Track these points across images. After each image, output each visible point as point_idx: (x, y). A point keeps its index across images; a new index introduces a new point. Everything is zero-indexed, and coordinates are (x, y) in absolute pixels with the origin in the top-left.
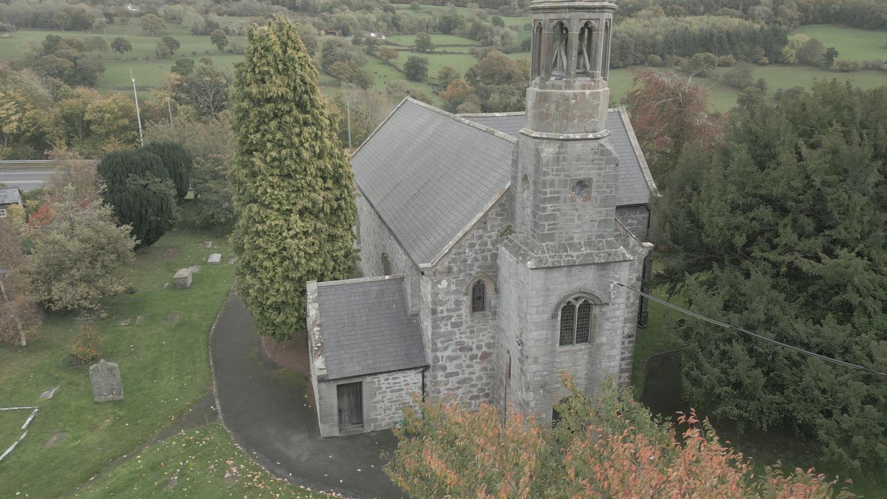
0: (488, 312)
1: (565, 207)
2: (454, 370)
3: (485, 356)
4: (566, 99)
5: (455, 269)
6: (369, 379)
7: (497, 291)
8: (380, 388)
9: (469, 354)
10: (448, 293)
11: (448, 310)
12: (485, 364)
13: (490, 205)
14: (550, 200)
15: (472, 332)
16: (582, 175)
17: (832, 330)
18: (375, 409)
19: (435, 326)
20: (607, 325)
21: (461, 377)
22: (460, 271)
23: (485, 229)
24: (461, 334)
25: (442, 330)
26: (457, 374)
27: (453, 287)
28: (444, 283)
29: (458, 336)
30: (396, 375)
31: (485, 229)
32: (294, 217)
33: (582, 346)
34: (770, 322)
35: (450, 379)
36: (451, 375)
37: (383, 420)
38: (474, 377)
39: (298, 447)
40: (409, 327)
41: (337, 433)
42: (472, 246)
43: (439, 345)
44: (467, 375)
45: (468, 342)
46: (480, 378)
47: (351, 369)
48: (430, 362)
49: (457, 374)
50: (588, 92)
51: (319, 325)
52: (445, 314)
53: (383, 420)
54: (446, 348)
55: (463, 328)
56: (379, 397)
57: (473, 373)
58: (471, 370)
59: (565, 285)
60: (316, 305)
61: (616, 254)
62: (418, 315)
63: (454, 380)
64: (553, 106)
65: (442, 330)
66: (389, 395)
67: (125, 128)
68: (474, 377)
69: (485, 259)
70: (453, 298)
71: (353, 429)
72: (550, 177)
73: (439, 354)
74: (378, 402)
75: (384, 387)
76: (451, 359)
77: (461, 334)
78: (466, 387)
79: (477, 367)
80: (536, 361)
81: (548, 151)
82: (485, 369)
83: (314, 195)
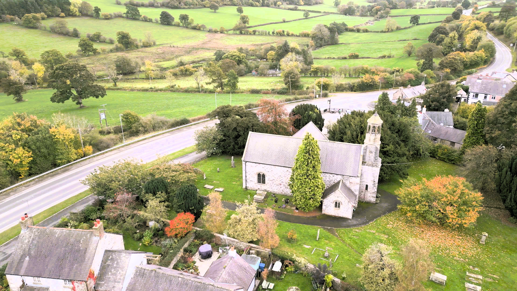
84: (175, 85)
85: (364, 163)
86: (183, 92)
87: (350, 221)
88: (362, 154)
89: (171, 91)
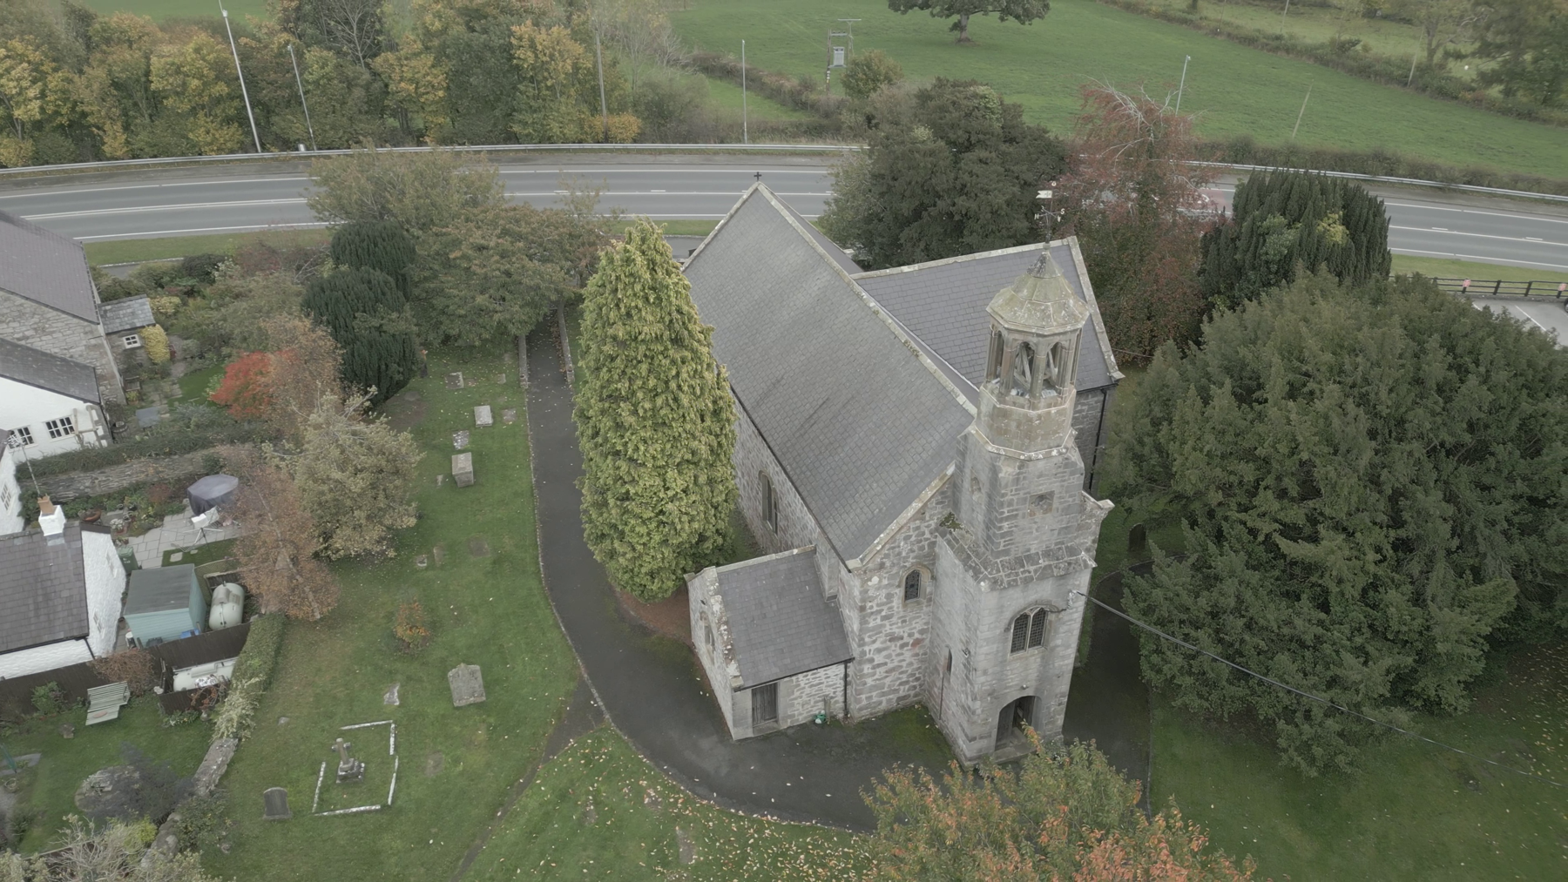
1: (1022, 522)
3: (917, 642)
4: (1030, 420)
5: (888, 564)
7: (934, 578)
10: (878, 589)
12: (917, 650)
13: (930, 494)
14: (1007, 519)
16: (1043, 490)
17: (1305, 618)
19: (863, 621)
20: (1063, 629)
21: (890, 666)
22: (893, 565)
23: (923, 519)
25: (871, 625)
27: (885, 582)
28: (875, 579)
31: (923, 519)
32: (671, 474)
33: (1035, 651)
34: (1240, 609)
36: (879, 665)
39: (709, 754)
40: (829, 611)
41: (750, 734)
42: (907, 538)
45: (897, 631)
46: (911, 664)
47: (767, 674)
48: (856, 654)
50: (1053, 410)
51: (726, 623)
55: (894, 619)
56: (797, 694)
59: (1019, 600)
60: (719, 598)
61: (1077, 562)
62: (835, 597)
63: (883, 669)
64: (1014, 425)
65: (871, 625)
66: (808, 690)
67: (218, 100)
69: (922, 548)
70: (884, 592)
71: (768, 725)
72: (1008, 498)
73: (867, 648)
76: (879, 651)
78: (895, 675)
79: (908, 654)
80: (985, 672)
81: (1007, 471)
83: (695, 444)
84: (1354, 44)
85: (949, 522)
86: (1350, 71)
87: (706, 743)
88: (951, 470)
89: (1322, 61)
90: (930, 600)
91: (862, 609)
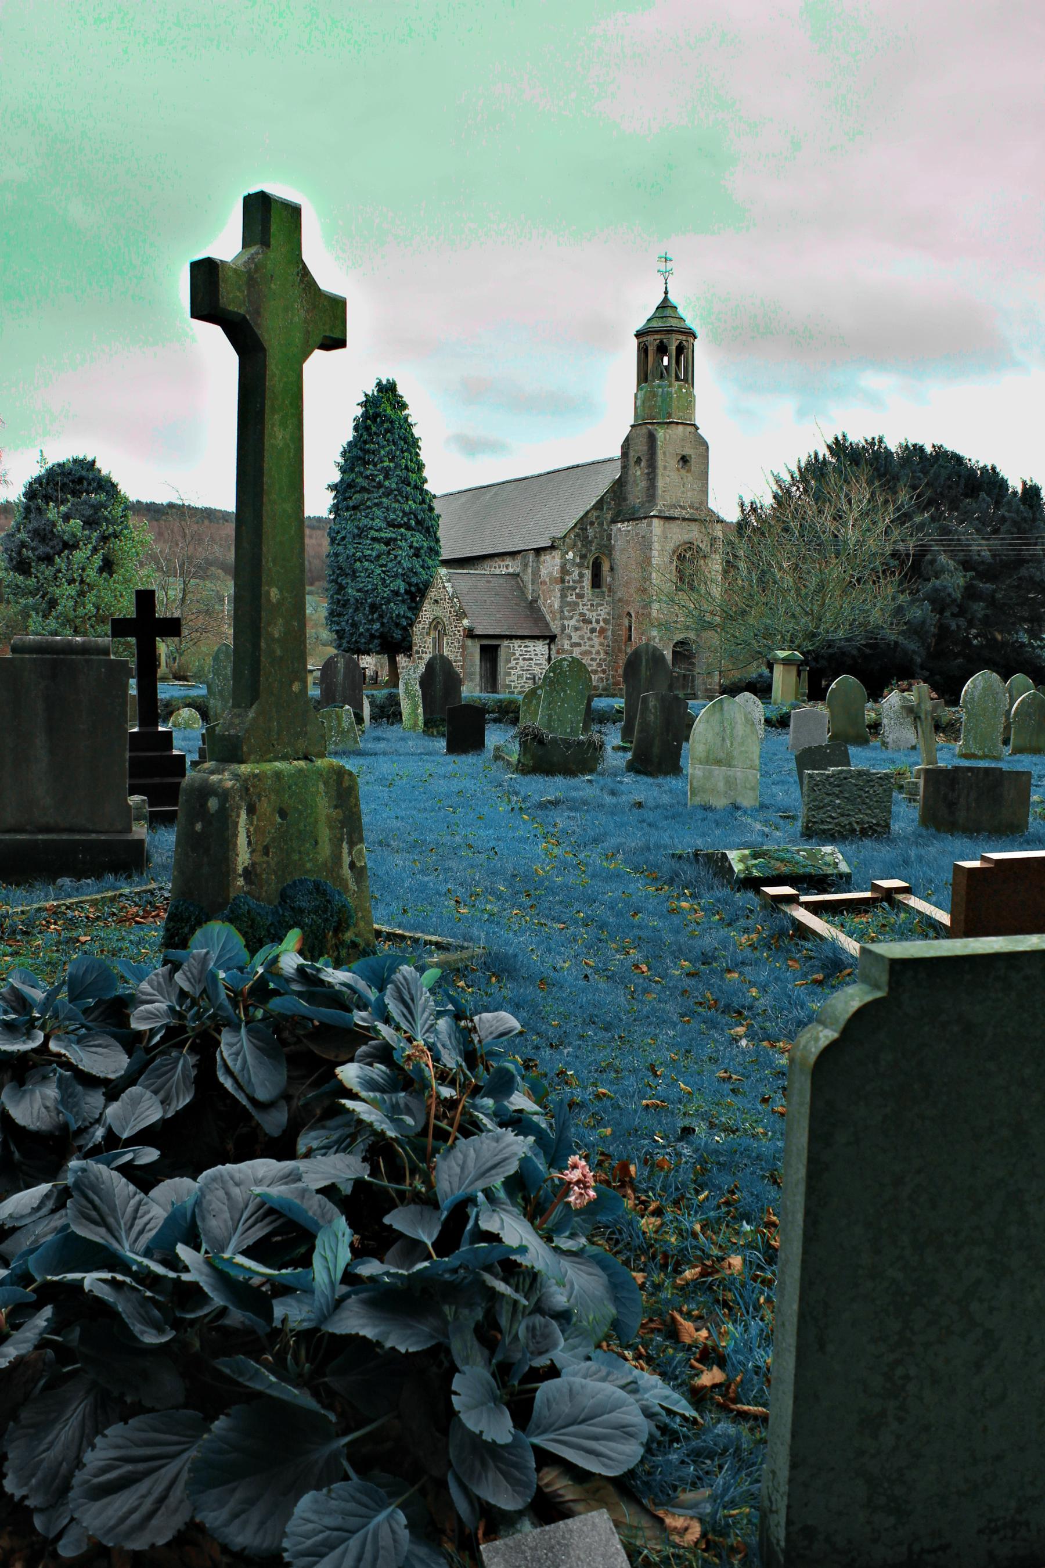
0: (605, 589)
2: (578, 641)
3: (602, 631)
6: (506, 643)
7: (612, 569)
8: (514, 654)
9: (590, 626)
11: (574, 582)
15: (592, 605)
18: (509, 674)
19: (563, 596)
21: (583, 648)
24: (584, 605)
25: (569, 599)
26: (579, 645)
29: (581, 607)
30: (527, 642)
35: (575, 649)
37: (516, 687)
38: (594, 651)
43: (566, 613)
44: (587, 648)
45: (589, 615)
46: (598, 653)
49: (579, 645)
52: (571, 584)
53: (516, 687)
54: (571, 618)
55: (585, 599)
57: (593, 647)
58: (591, 643)
68: (594, 651)
73: (566, 622)
74: (512, 668)
75: (518, 653)
77: (584, 605)
79: (596, 641)
82: (601, 644)
90: (610, 590)
91: (563, 581)
